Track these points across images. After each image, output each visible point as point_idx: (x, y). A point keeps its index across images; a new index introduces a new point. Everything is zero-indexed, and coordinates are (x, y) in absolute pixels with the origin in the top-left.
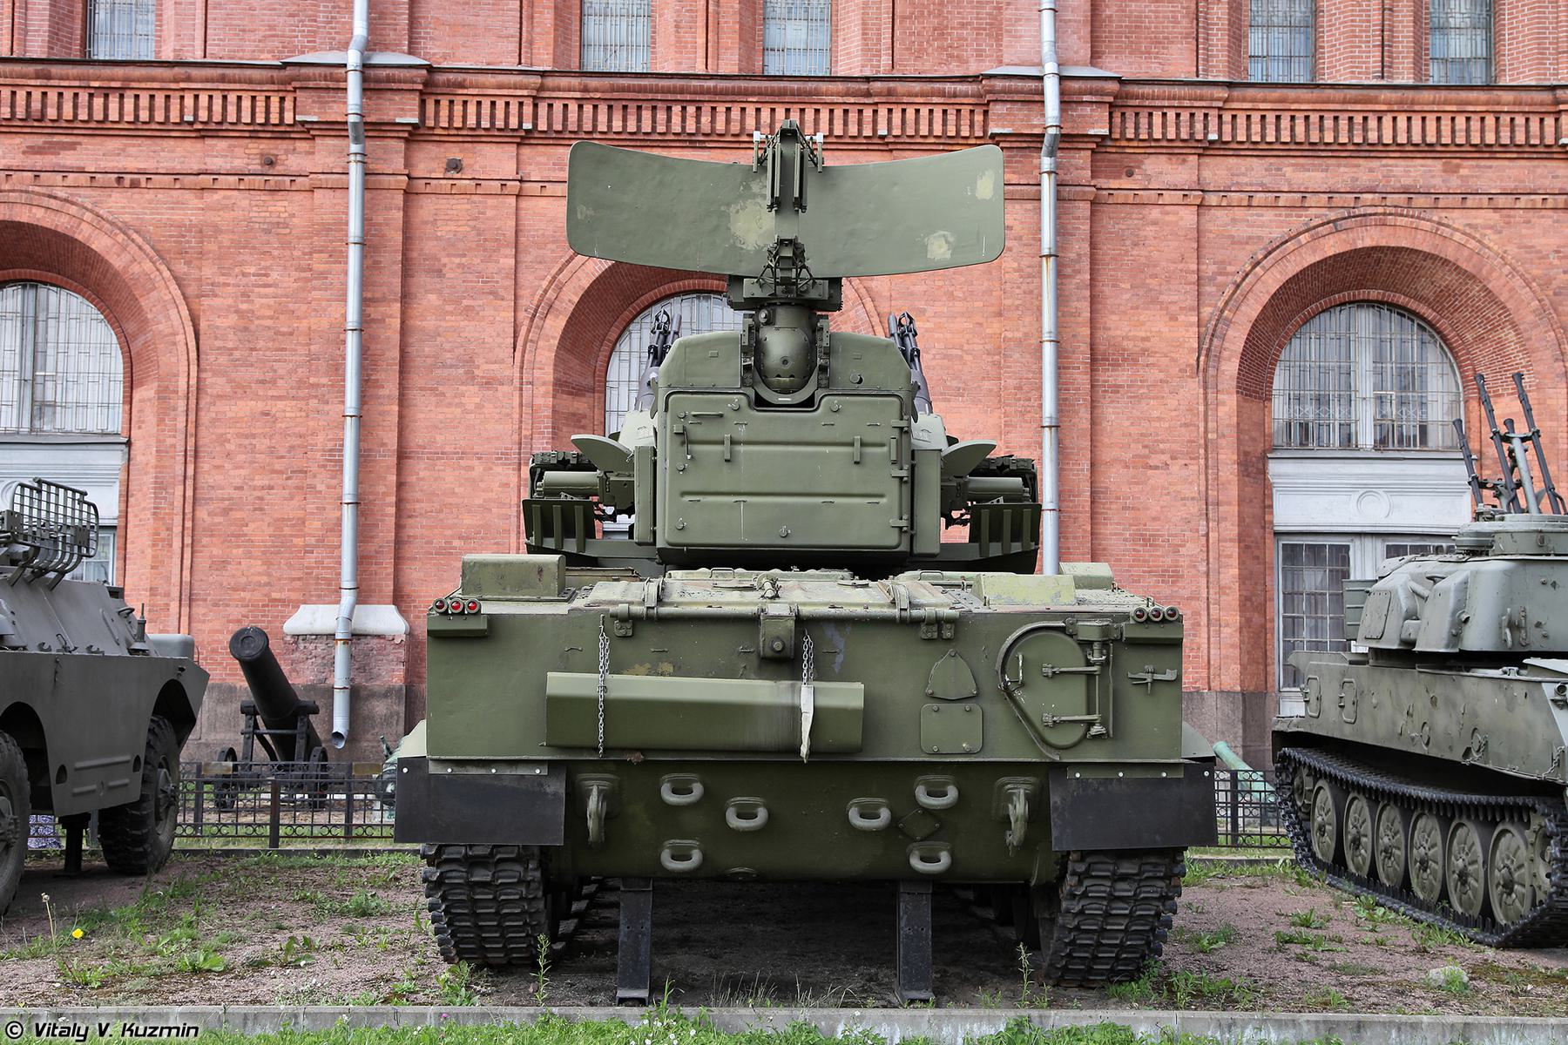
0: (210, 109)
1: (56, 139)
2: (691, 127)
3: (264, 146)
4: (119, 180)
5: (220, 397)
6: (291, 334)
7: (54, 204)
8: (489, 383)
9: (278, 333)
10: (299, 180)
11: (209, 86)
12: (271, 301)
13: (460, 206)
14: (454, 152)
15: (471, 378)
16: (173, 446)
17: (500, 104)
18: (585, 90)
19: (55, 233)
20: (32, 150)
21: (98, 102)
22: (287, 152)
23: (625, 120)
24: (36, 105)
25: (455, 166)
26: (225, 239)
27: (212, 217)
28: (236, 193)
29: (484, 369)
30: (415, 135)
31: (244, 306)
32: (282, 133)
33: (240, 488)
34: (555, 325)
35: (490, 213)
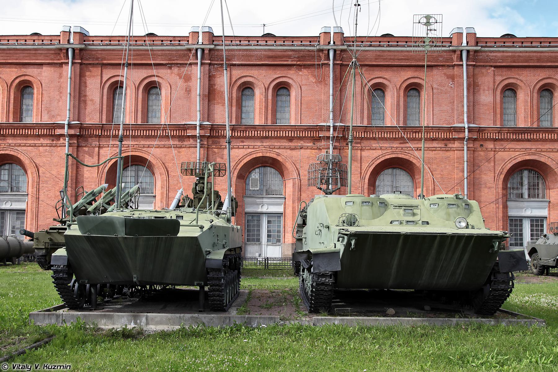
2: (529, 138)
3: (445, 142)
8: (489, 188)
13: (482, 153)
14: (482, 143)
15: (486, 187)
19: (406, 159)
20: (401, 143)
21: (414, 134)
25: (482, 145)
26: (438, 160)
27: (435, 156)
29: (488, 185)
30: (475, 140)
32: (449, 140)
34: (502, 177)
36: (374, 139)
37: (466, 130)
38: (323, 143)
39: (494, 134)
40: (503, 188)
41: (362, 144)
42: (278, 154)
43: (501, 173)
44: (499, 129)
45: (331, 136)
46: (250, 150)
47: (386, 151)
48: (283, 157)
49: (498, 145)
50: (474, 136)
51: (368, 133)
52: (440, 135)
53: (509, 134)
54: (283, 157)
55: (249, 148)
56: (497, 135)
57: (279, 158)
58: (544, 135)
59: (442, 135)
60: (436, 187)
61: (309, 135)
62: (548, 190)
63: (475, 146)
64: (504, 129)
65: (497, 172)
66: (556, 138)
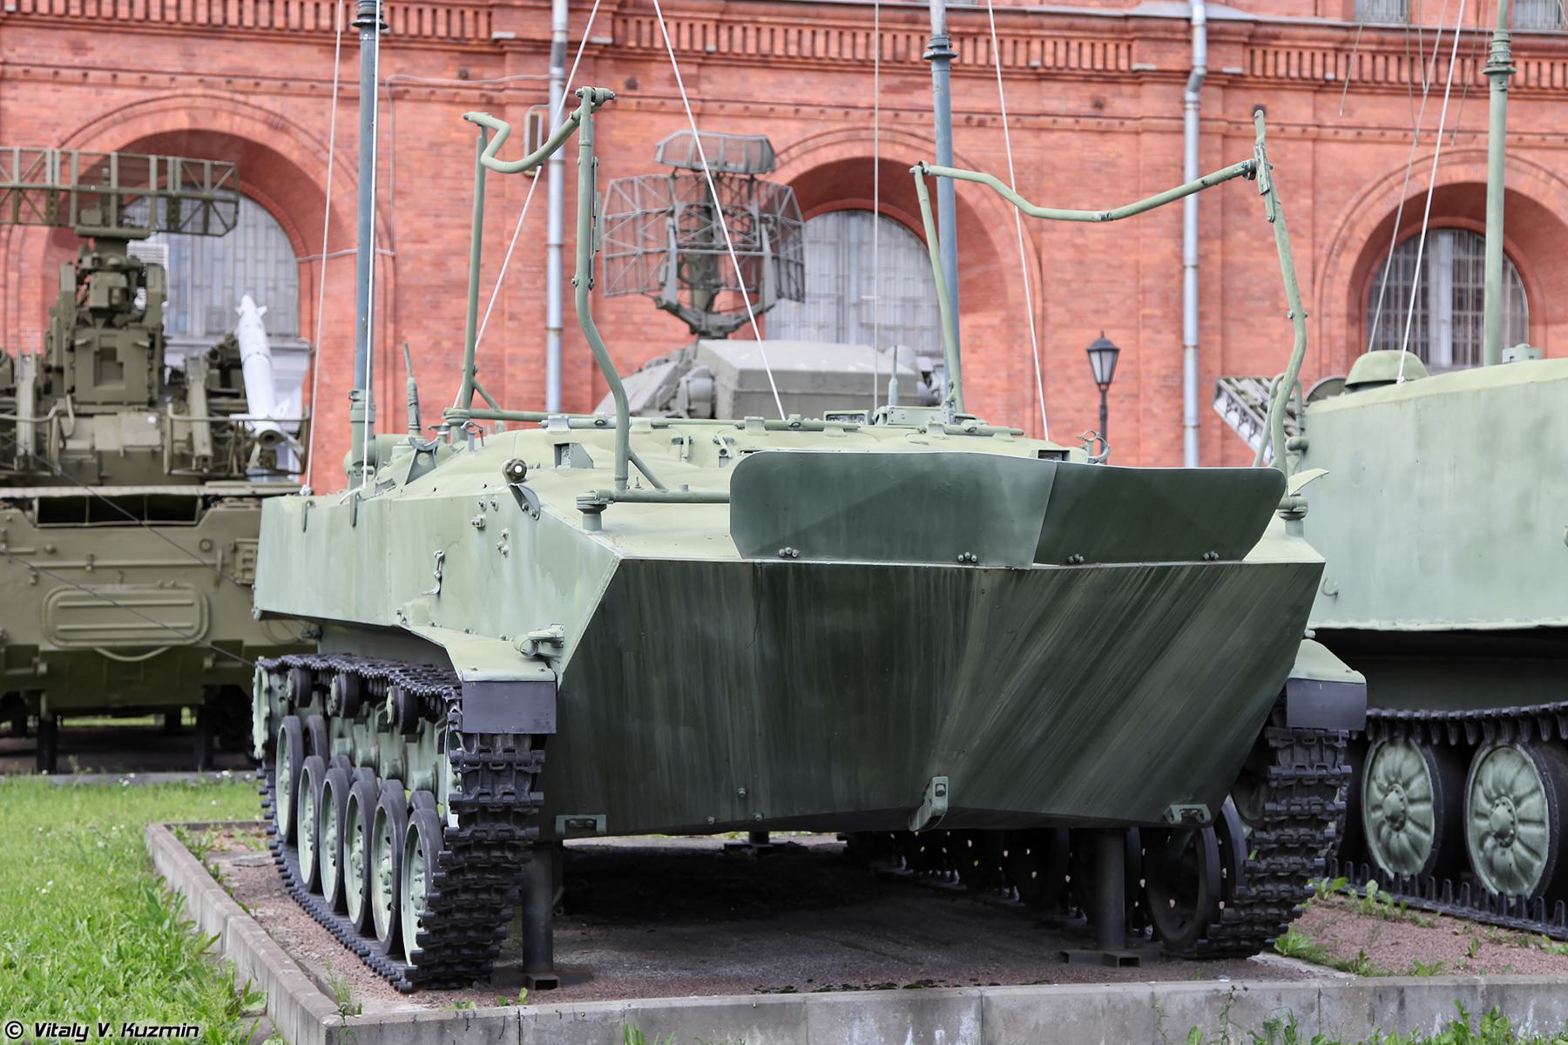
0: (1055, 54)
1: (910, 79)
4: (968, 119)
5: (1061, 326)
6: (1120, 267)
7: (914, 142)
9: (1110, 266)
10: (1128, 122)
11: (1056, 33)
12: (1102, 236)
14: (1259, 98)
16: (1022, 371)
17: (1307, 55)
18: (1382, 43)
22: (1114, 95)
23: (1412, 70)
24: (901, 48)
28: (1069, 134)
30: (1233, 83)
31: (1079, 241)
32: (1110, 78)
33: (1079, 411)
34: (1348, 262)
35: (1290, 156)
36: (765, 62)
37: (1199, 36)
38: (510, 75)
39: (1319, 58)
40: (1349, 315)
41: (705, 87)
42: (279, 125)
43: (1344, 245)
44: (1342, 34)
45: (559, 38)
46: (119, 96)
47: (818, 128)
48: (304, 139)
49: (1335, 110)
50: (1229, 62)
51: (738, 31)
52: (1074, 55)
53: (1380, 60)
54: (304, 139)
55: (114, 83)
56: (1330, 60)
57: (282, 145)
58: (1533, 68)
59: (1086, 57)
60: (1051, 309)
61: (442, 31)
62: (1539, 329)
63: (1232, 114)
64: (1360, 35)
65: (1328, 241)
66: (1558, 82)
